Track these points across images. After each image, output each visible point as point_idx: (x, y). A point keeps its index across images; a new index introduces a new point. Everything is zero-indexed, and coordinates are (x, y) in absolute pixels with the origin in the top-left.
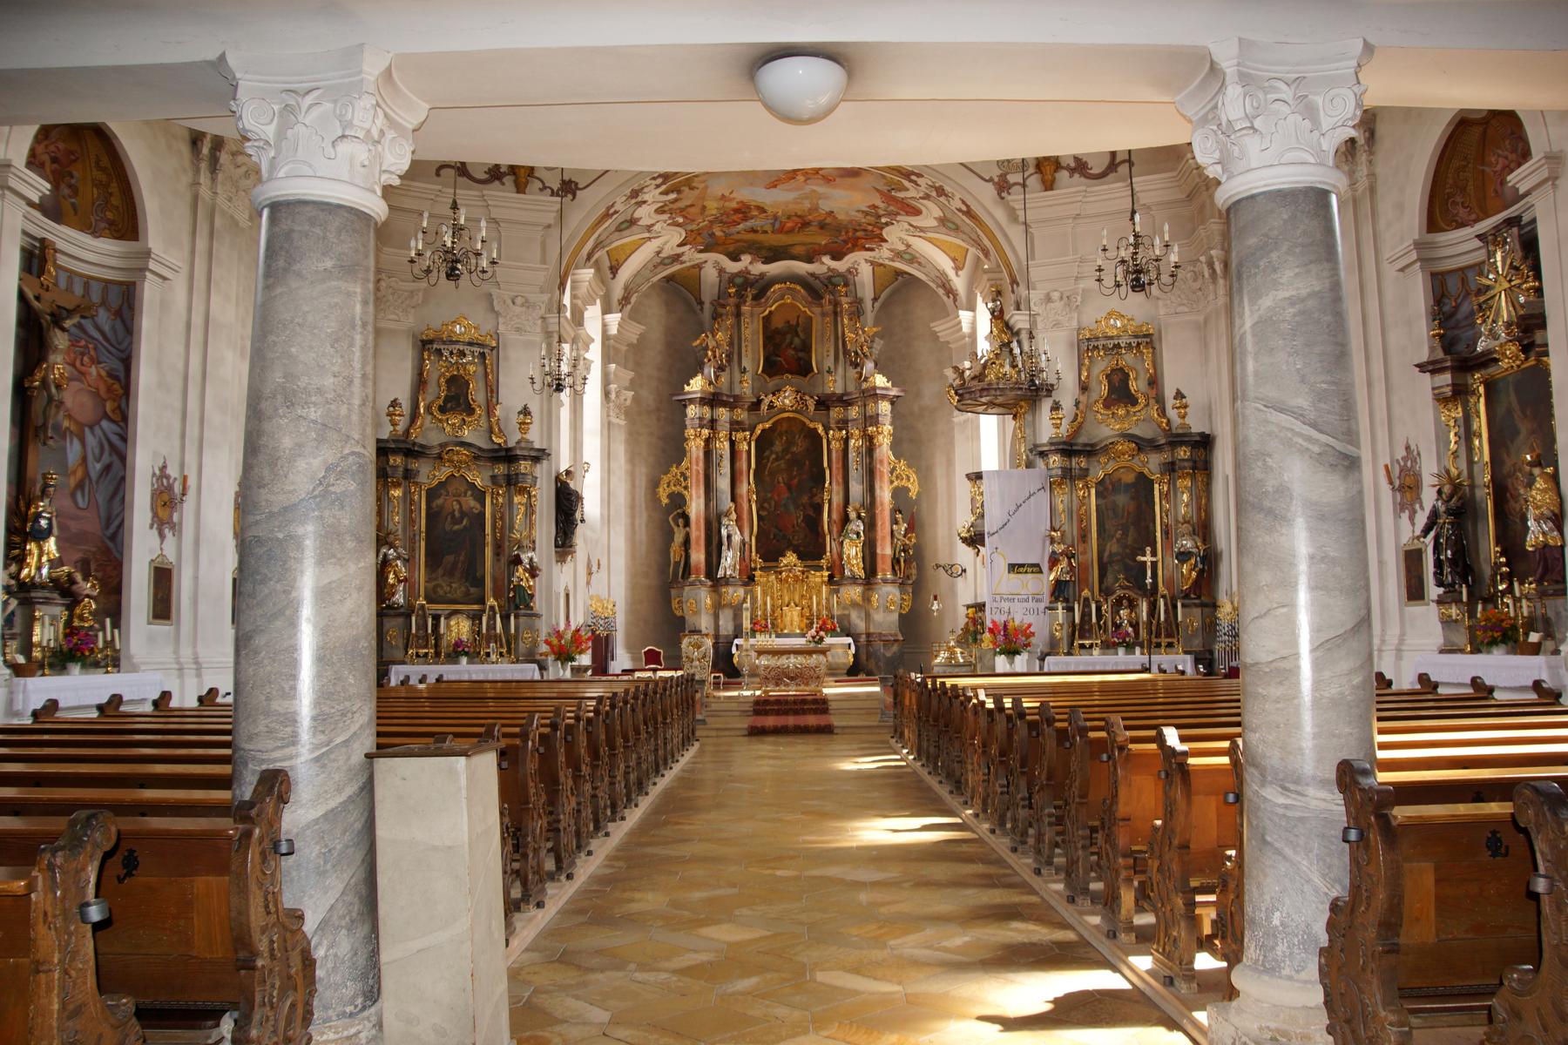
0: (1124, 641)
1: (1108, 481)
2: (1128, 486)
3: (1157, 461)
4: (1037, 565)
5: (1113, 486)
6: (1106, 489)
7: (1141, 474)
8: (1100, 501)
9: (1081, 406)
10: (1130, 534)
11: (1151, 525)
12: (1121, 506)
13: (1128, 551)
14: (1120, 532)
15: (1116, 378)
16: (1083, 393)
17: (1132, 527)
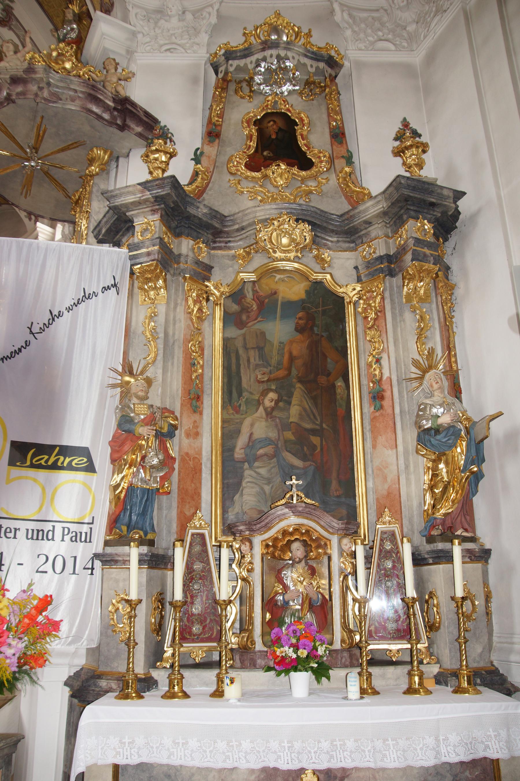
0: (312, 655)
1: (250, 295)
2: (288, 305)
3: (351, 264)
4: (85, 452)
5: (261, 304)
6: (245, 309)
7: (318, 285)
8: (234, 332)
9: (204, 160)
10: (295, 401)
11: (340, 383)
12: (276, 343)
13: (289, 435)
14: (272, 395)
15: (272, 128)
16: (211, 142)
17: (298, 385)
